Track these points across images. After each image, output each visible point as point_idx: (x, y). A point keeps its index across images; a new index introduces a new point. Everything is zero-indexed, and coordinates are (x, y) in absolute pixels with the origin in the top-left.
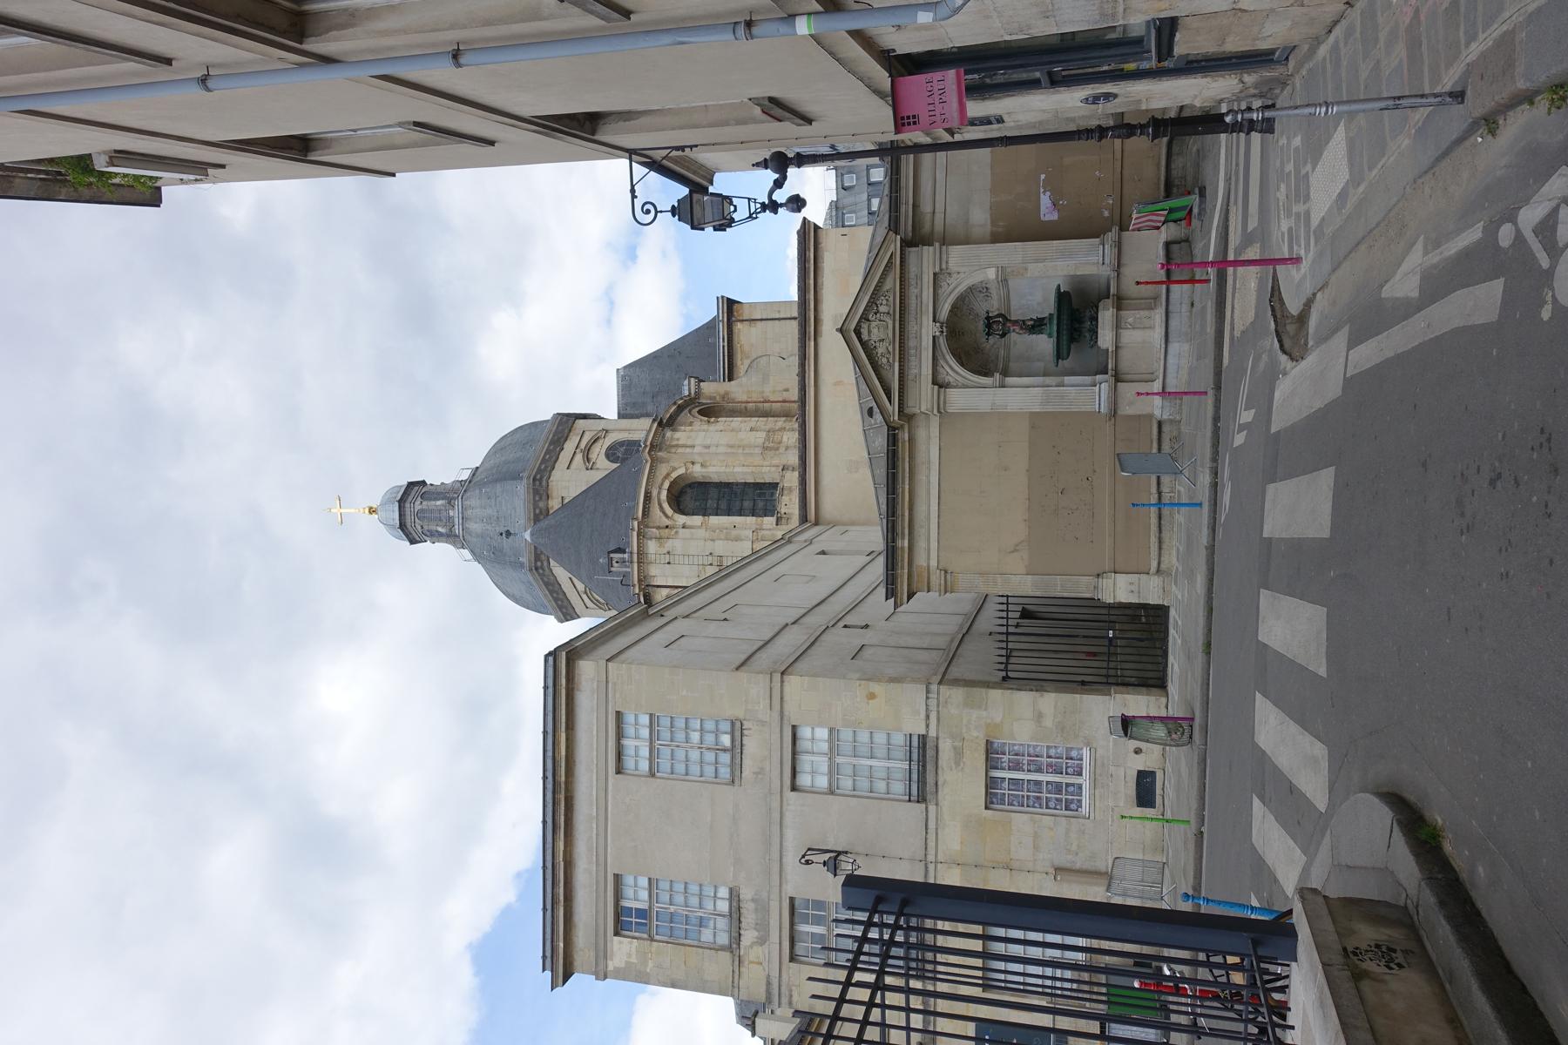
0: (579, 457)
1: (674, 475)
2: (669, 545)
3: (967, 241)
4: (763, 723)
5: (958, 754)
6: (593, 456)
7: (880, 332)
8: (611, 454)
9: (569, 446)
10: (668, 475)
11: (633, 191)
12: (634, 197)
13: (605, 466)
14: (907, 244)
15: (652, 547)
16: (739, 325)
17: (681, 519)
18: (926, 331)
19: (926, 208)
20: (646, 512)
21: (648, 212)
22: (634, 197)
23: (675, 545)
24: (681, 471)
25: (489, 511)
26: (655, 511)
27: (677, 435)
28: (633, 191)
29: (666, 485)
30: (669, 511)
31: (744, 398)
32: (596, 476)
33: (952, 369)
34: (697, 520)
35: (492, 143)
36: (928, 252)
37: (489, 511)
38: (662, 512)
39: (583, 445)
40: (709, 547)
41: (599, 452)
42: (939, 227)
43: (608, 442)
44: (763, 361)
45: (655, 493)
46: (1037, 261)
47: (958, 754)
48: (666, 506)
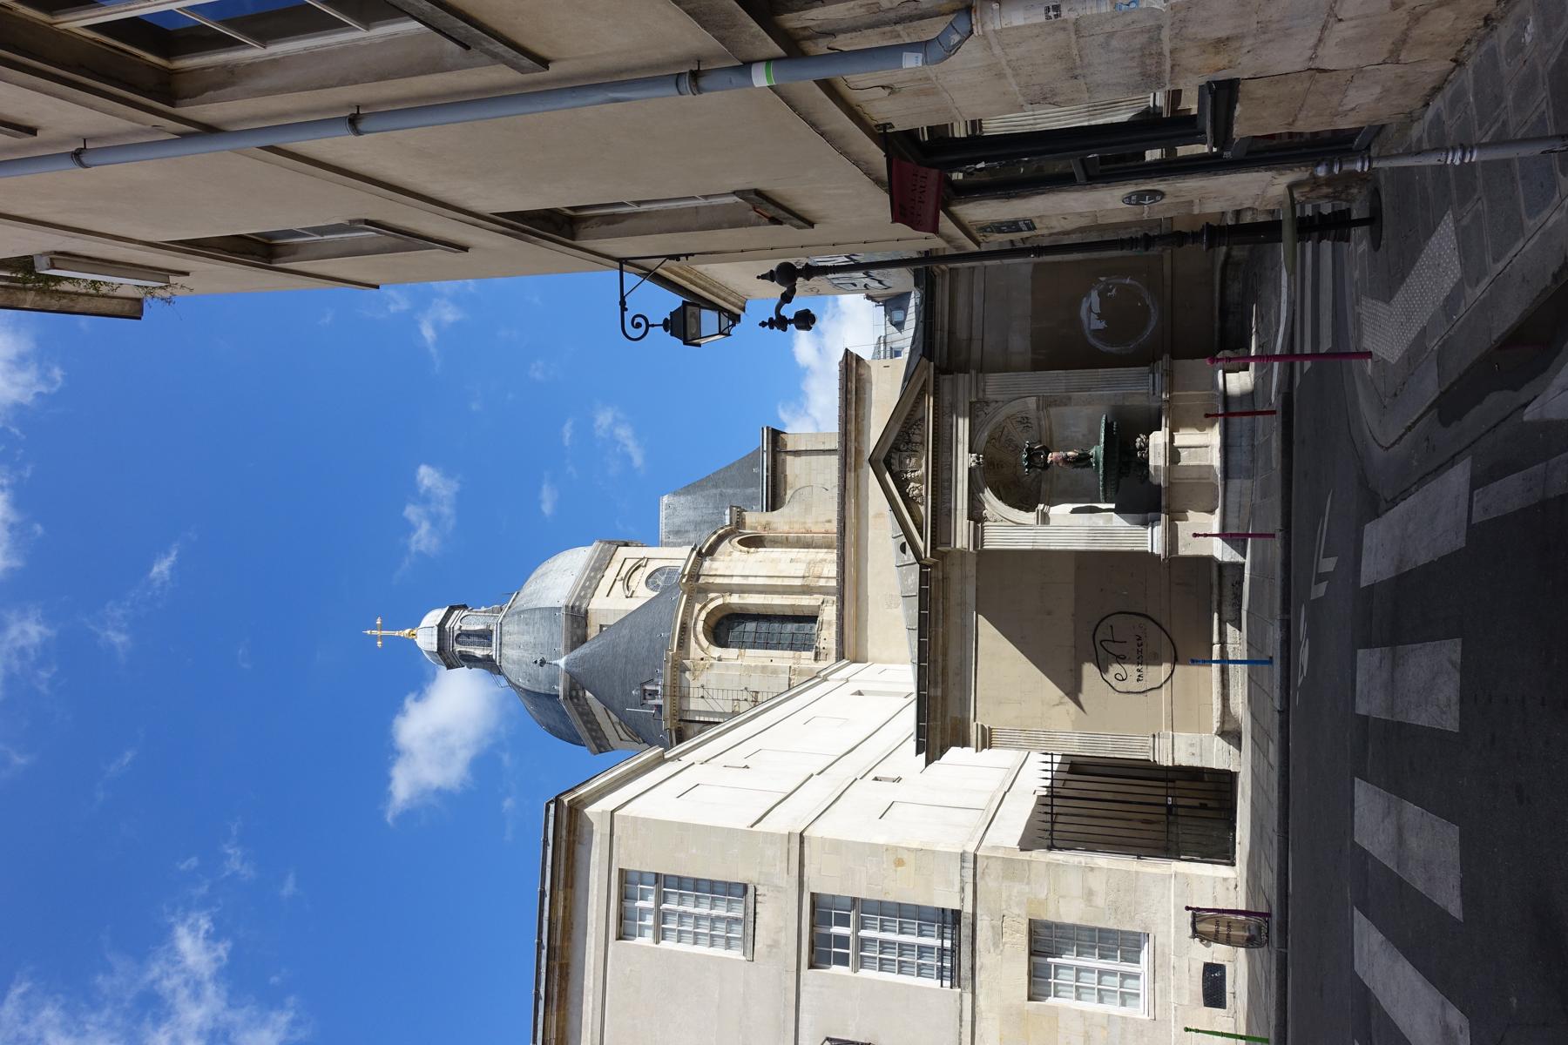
0: (619, 584)
3: (1005, 368)
4: (778, 889)
5: (999, 933)
8: (650, 580)
9: (610, 574)
11: (623, 303)
12: (624, 309)
13: (644, 594)
14: (940, 371)
17: (716, 651)
19: (962, 334)
21: (639, 325)
22: (624, 309)
25: (526, 638)
27: (716, 565)
28: (623, 303)
30: (705, 643)
31: (786, 528)
32: (634, 604)
33: (993, 505)
35: (465, 249)
36: (963, 379)
37: (526, 638)
41: (640, 577)
42: (976, 354)
44: (806, 491)
46: (1081, 390)
47: (999, 933)
48: (701, 637)
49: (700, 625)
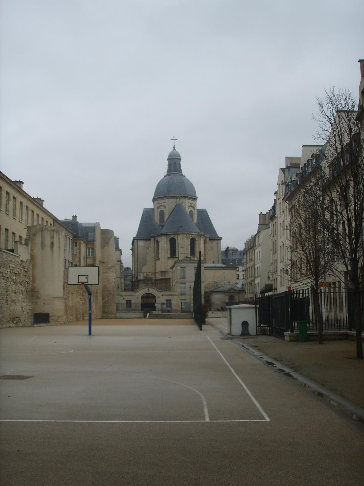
0: (190, 205)
1: (196, 238)
7: (232, 291)
10: (196, 237)
13: (188, 211)
15: (185, 235)
16: (217, 241)
17: (189, 240)
18: (232, 294)
20: (190, 234)
23: (186, 240)
24: (197, 240)
26: (190, 236)
29: (194, 237)
33: (229, 296)
34: (189, 243)
38: (190, 237)
39: (192, 205)
41: (191, 209)
43: (193, 210)
45: (193, 235)
48: (191, 237)
49: (193, 237)
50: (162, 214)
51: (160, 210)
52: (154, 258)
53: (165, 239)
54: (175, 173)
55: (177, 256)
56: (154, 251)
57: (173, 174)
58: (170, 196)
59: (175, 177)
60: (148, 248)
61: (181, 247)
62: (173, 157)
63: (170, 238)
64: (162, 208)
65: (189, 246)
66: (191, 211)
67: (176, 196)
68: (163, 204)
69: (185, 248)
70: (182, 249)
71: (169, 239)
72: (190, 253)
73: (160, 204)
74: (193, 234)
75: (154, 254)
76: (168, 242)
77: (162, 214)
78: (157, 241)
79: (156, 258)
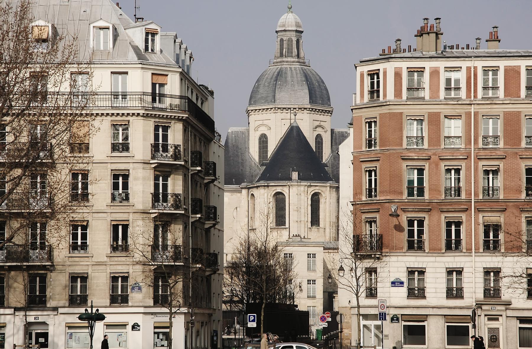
0: (317, 123)
1: (322, 193)
2: (302, 194)
6: (317, 129)
15: (302, 188)
23: (303, 197)
24: (324, 195)
27: (334, 193)
29: (319, 191)
34: (310, 202)
40: (302, 207)
41: (319, 131)
45: (317, 188)
49: (317, 191)
50: (263, 140)
51: (258, 134)
52: (246, 226)
53: (266, 195)
54: (289, 59)
55: (287, 226)
56: (247, 213)
57: (287, 62)
58: (278, 108)
59: (289, 69)
60: (237, 208)
61: (294, 210)
62: (287, 29)
63: (274, 192)
64: (263, 130)
65: (310, 208)
66: (319, 139)
67: (289, 108)
68: (265, 122)
69: (302, 211)
70: (296, 213)
71: (273, 193)
72: (310, 220)
73: (261, 122)
74: (316, 186)
75: (247, 219)
76: (272, 199)
77: (263, 140)
78: (252, 195)
79: (250, 228)
